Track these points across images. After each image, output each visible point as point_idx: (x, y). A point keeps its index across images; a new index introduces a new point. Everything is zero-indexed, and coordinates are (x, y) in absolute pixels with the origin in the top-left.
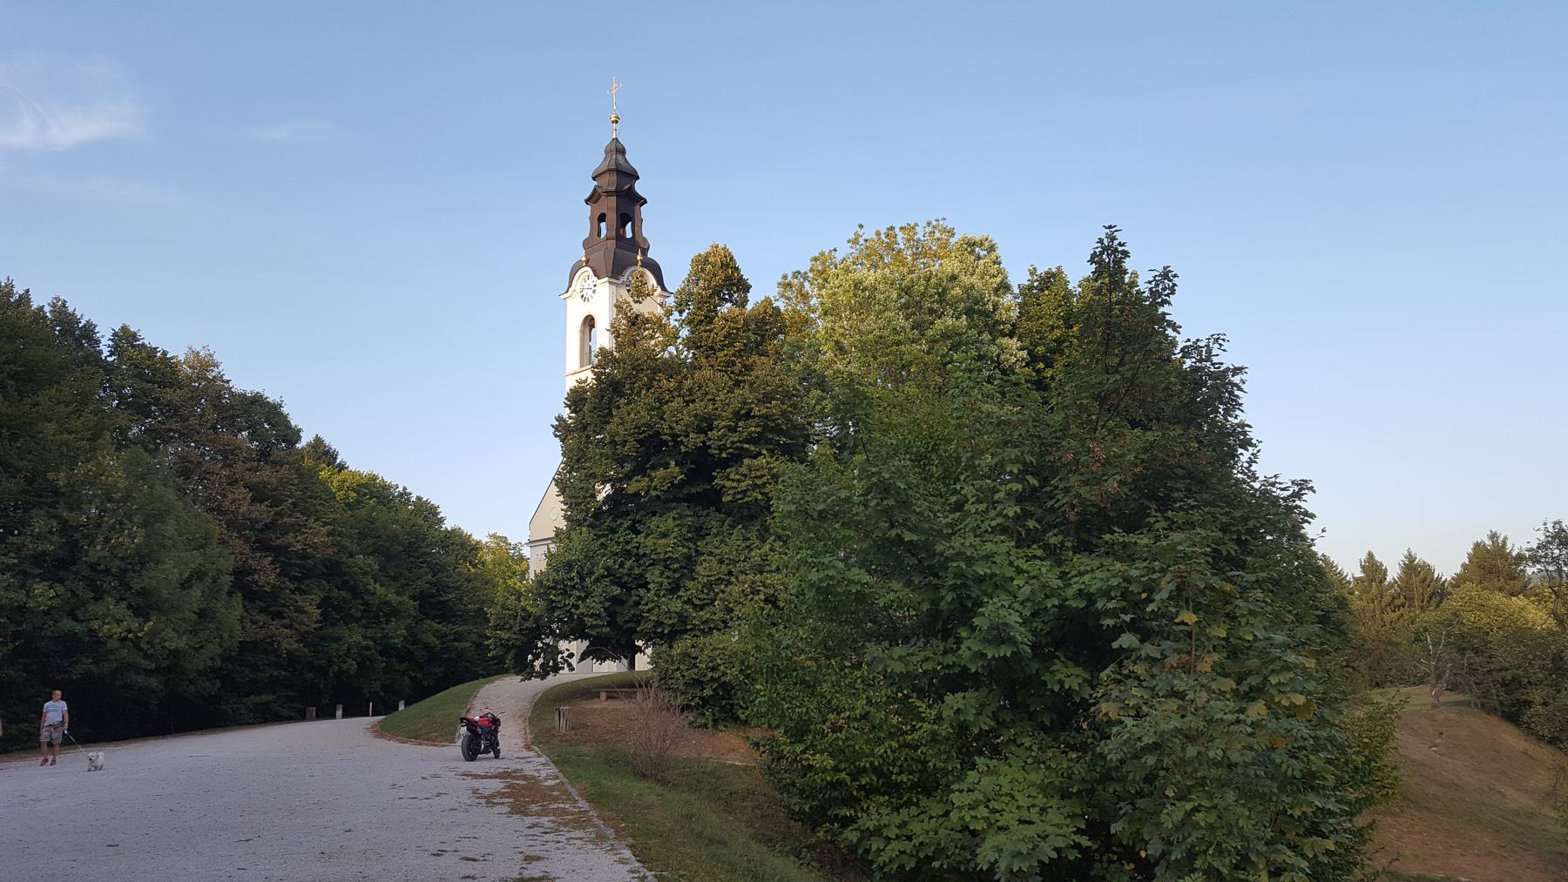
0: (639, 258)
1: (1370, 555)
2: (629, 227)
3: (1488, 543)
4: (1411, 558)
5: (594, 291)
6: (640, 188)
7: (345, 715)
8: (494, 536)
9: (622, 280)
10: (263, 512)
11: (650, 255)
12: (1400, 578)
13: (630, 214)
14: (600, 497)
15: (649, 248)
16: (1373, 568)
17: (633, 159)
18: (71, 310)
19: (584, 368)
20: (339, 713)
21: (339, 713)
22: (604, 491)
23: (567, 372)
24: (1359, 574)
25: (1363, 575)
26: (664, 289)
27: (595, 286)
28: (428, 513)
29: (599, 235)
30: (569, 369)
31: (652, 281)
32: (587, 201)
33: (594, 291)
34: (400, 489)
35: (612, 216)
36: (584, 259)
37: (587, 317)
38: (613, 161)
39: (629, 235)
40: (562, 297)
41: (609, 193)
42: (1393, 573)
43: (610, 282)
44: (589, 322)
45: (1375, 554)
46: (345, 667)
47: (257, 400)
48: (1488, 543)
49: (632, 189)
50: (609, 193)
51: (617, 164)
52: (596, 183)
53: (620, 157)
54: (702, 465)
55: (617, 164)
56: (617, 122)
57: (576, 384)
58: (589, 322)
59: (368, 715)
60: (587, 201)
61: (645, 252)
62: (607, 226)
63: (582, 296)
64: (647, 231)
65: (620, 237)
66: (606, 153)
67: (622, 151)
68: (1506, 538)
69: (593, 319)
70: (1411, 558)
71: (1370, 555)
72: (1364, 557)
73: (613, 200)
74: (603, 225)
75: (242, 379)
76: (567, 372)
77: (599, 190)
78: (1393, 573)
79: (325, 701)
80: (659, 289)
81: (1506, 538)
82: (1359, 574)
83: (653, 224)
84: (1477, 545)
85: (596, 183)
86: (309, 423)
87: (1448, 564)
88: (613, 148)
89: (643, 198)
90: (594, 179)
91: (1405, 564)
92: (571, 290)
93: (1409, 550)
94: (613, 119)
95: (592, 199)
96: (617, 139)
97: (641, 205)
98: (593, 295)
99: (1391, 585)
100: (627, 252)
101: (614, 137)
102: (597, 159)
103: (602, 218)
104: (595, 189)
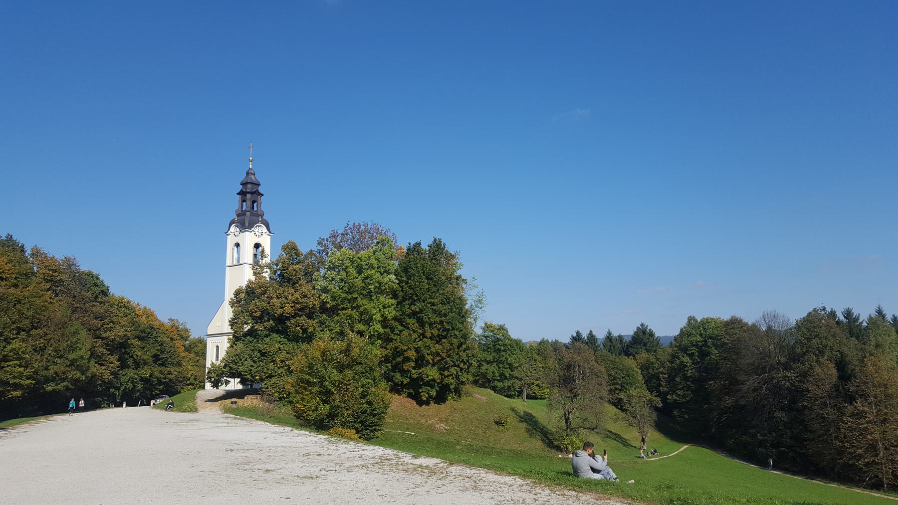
1: (591, 331)
2: (255, 205)
3: (641, 327)
4: (609, 333)
6: (261, 189)
7: (127, 406)
8: (170, 320)
9: (252, 229)
10: (98, 323)
14: (246, 330)
16: (591, 335)
17: (259, 177)
18: (14, 239)
20: (124, 405)
21: (124, 405)
22: (247, 328)
23: (227, 265)
26: (270, 232)
28: (149, 315)
29: (242, 208)
31: (265, 229)
32: (238, 194)
34: (136, 303)
35: (249, 203)
37: (236, 244)
39: (255, 209)
44: (237, 245)
45: (593, 331)
46: (127, 387)
47: (89, 274)
49: (257, 190)
50: (249, 193)
53: (253, 176)
54: (281, 320)
57: (239, 287)
59: (137, 406)
60: (238, 194)
61: (262, 216)
64: (264, 207)
67: (254, 174)
68: (647, 326)
70: (609, 333)
71: (591, 331)
72: (588, 332)
74: (244, 203)
75: (84, 265)
76: (227, 265)
79: (118, 401)
80: (268, 232)
81: (647, 326)
83: (265, 204)
86: (118, 289)
90: (241, 184)
92: (229, 232)
93: (609, 330)
95: (242, 193)
101: (251, 167)
103: (244, 201)
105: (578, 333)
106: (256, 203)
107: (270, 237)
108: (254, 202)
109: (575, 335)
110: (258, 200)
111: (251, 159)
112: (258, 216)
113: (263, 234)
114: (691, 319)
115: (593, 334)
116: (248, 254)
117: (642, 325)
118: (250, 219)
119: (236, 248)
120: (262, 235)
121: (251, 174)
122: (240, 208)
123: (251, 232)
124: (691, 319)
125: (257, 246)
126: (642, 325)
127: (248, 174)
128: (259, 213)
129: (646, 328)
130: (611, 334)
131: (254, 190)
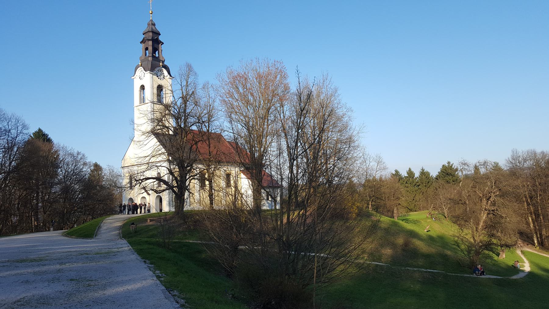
0: (161, 64)
1: (410, 169)
2: (157, 52)
3: (447, 165)
4: (423, 170)
5: (144, 76)
6: (161, 38)
11: (165, 63)
12: (420, 177)
13: (157, 48)
15: (165, 60)
16: (410, 173)
17: (158, 28)
19: (141, 104)
24: (407, 175)
25: (407, 175)
26: (170, 76)
27: (144, 74)
29: (146, 55)
30: (135, 106)
33: (144, 76)
35: (150, 48)
36: (140, 64)
38: (150, 28)
40: (132, 78)
41: (149, 40)
42: (417, 175)
43: (150, 73)
44: (143, 87)
48: (447, 165)
49: (157, 39)
51: (152, 29)
52: (144, 36)
53: (153, 27)
55: (152, 29)
56: (152, 14)
58: (143, 87)
60: (141, 43)
61: (163, 62)
62: (149, 52)
63: (140, 78)
65: (154, 57)
66: (148, 25)
67: (154, 25)
69: (144, 86)
70: (423, 170)
71: (410, 169)
72: (408, 169)
73: (150, 43)
74: (147, 51)
77: (145, 38)
78: (417, 175)
80: (169, 76)
82: (406, 175)
84: (443, 166)
85: (144, 36)
87: (434, 172)
88: (151, 23)
89: (161, 42)
90: (143, 34)
91: (421, 172)
94: (151, 12)
95: (143, 42)
96: (152, 20)
97: (161, 45)
98: (144, 77)
99: (416, 178)
100: (157, 62)
101: (151, 19)
102: (145, 28)
104: (144, 38)
105: (396, 171)
106: (157, 52)
107: (171, 80)
108: (155, 49)
109: (394, 173)
110: (158, 47)
111: (150, 11)
112: (159, 61)
113: (165, 78)
114: (514, 152)
115: (412, 170)
116: (149, 94)
117: (449, 163)
118: (152, 62)
119: (142, 91)
120: (164, 78)
121: (152, 24)
122: (144, 55)
123: (153, 74)
124: (514, 152)
125: (160, 88)
126: (449, 163)
127: (148, 24)
128: (161, 59)
129: (452, 165)
130: (424, 171)
131: (156, 38)
